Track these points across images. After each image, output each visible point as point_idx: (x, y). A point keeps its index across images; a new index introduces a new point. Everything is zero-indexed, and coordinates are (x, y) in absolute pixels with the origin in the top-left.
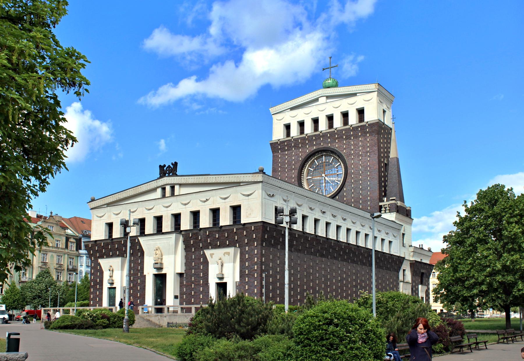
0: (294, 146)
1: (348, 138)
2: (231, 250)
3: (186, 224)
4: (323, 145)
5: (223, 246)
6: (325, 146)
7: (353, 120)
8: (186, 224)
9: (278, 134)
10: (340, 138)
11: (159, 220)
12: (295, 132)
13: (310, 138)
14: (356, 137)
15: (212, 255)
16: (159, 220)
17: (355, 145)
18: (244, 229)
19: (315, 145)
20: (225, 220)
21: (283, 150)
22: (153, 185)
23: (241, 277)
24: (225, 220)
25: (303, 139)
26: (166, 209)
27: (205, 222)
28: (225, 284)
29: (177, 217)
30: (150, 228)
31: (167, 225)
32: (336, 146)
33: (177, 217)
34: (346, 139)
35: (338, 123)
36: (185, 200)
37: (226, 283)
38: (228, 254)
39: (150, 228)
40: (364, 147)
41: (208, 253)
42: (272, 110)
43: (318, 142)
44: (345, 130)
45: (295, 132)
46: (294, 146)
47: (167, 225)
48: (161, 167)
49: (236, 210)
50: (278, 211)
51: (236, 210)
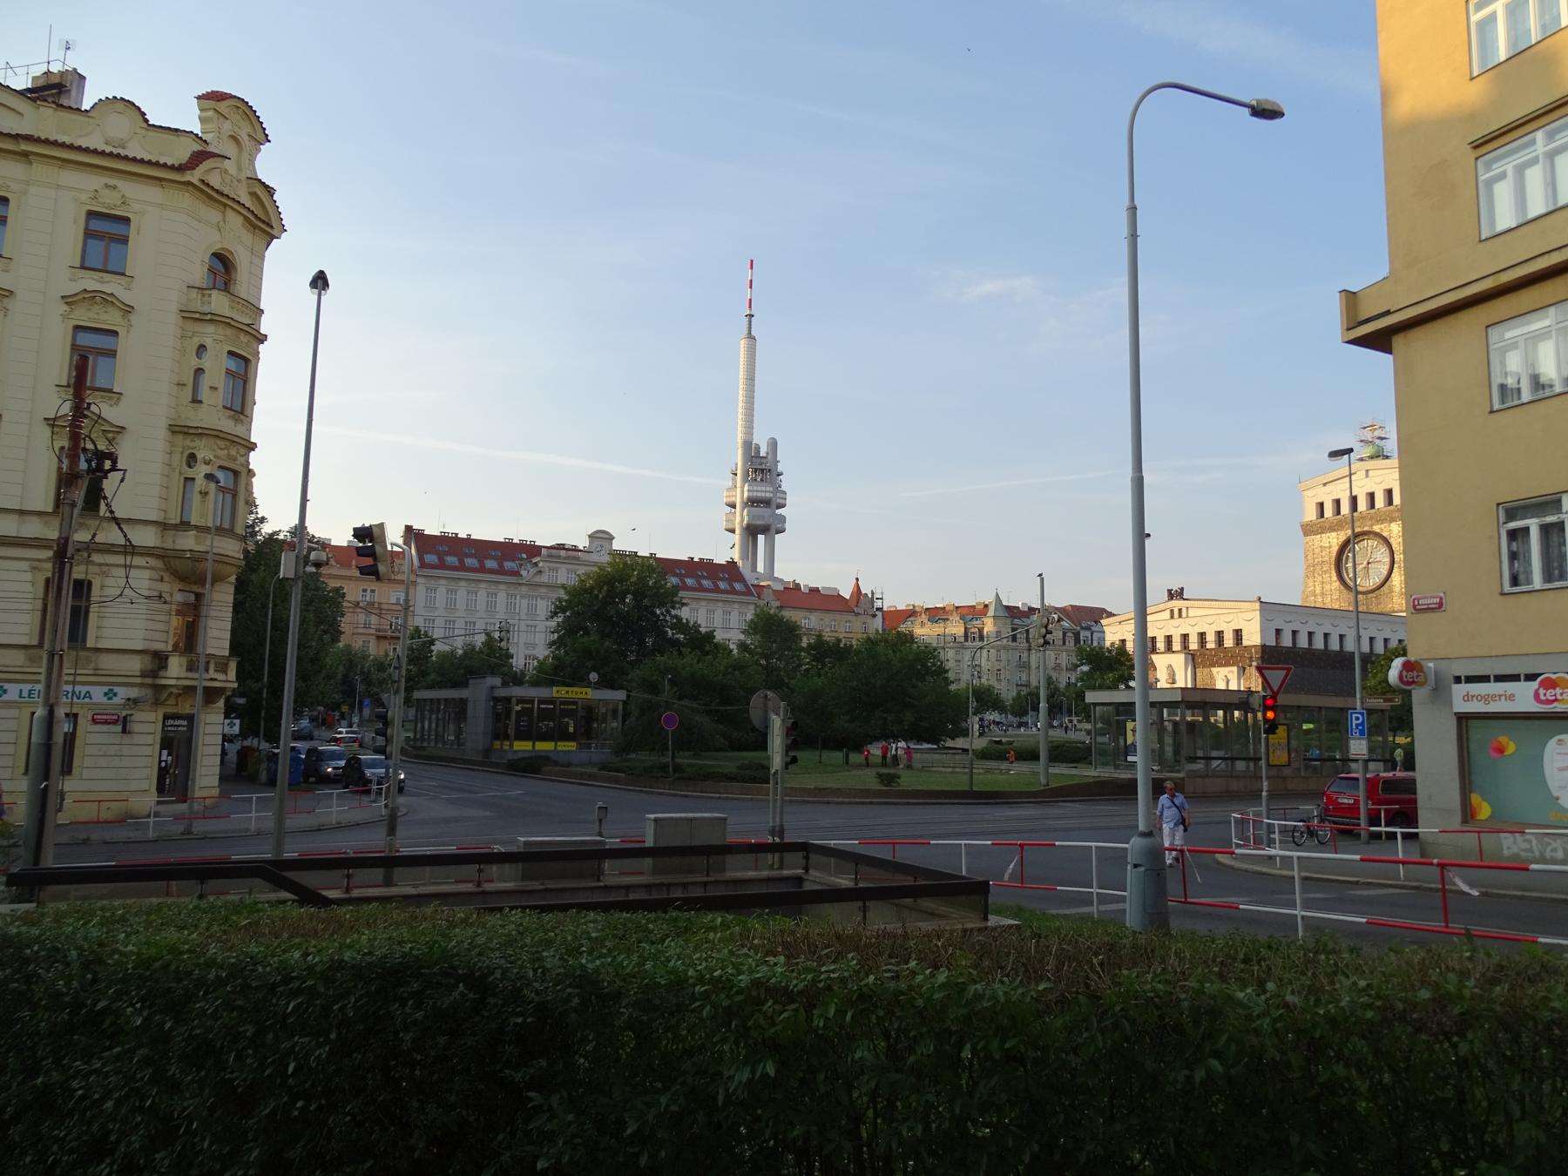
2: (1235, 669)
3: (1194, 646)
5: (1227, 664)
8: (1194, 646)
9: (1311, 515)
11: (1169, 639)
16: (1169, 639)
20: (1229, 642)
22: (1162, 607)
24: (1229, 642)
26: (1176, 629)
29: (1185, 637)
30: (1161, 645)
31: (1177, 646)
32: (1376, 528)
33: (1185, 637)
36: (1193, 622)
39: (1161, 645)
47: (1177, 646)
48: (1170, 591)
49: (1238, 634)
50: (1278, 631)
51: (1238, 634)
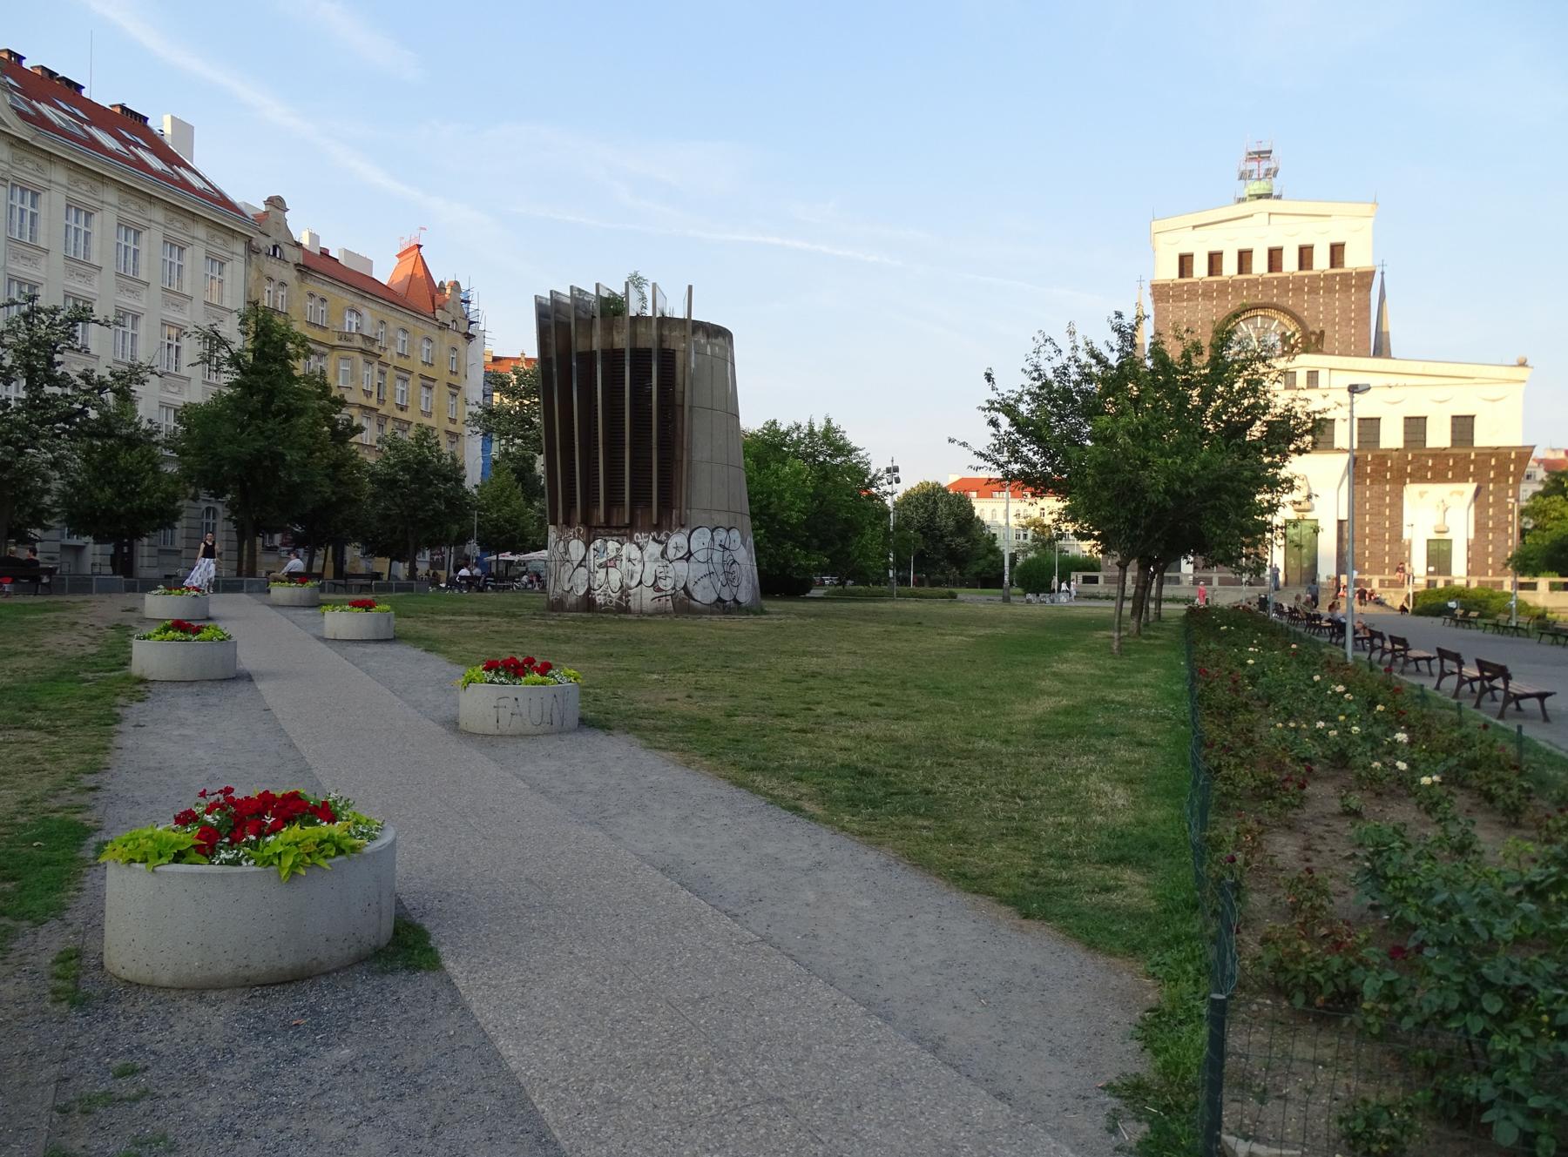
0: (1204, 295)
1: (1313, 291)
4: (1260, 299)
5: (1439, 477)
6: (1266, 300)
7: (1321, 262)
10: (1298, 290)
12: (1200, 269)
13: (1236, 286)
14: (1330, 290)
15: (1422, 494)
17: (1325, 304)
18: (1492, 455)
19: (1243, 297)
20: (1439, 436)
21: (1178, 298)
23: (1476, 531)
24: (1439, 436)
25: (1225, 284)
27: (1392, 437)
28: (1450, 541)
34: (1309, 293)
35: (1290, 263)
37: (1450, 541)
38: (1461, 493)
40: (1344, 311)
41: (1412, 491)
42: (1156, 226)
43: (1253, 292)
44: (1310, 277)
45: (1200, 269)
46: (1204, 295)
